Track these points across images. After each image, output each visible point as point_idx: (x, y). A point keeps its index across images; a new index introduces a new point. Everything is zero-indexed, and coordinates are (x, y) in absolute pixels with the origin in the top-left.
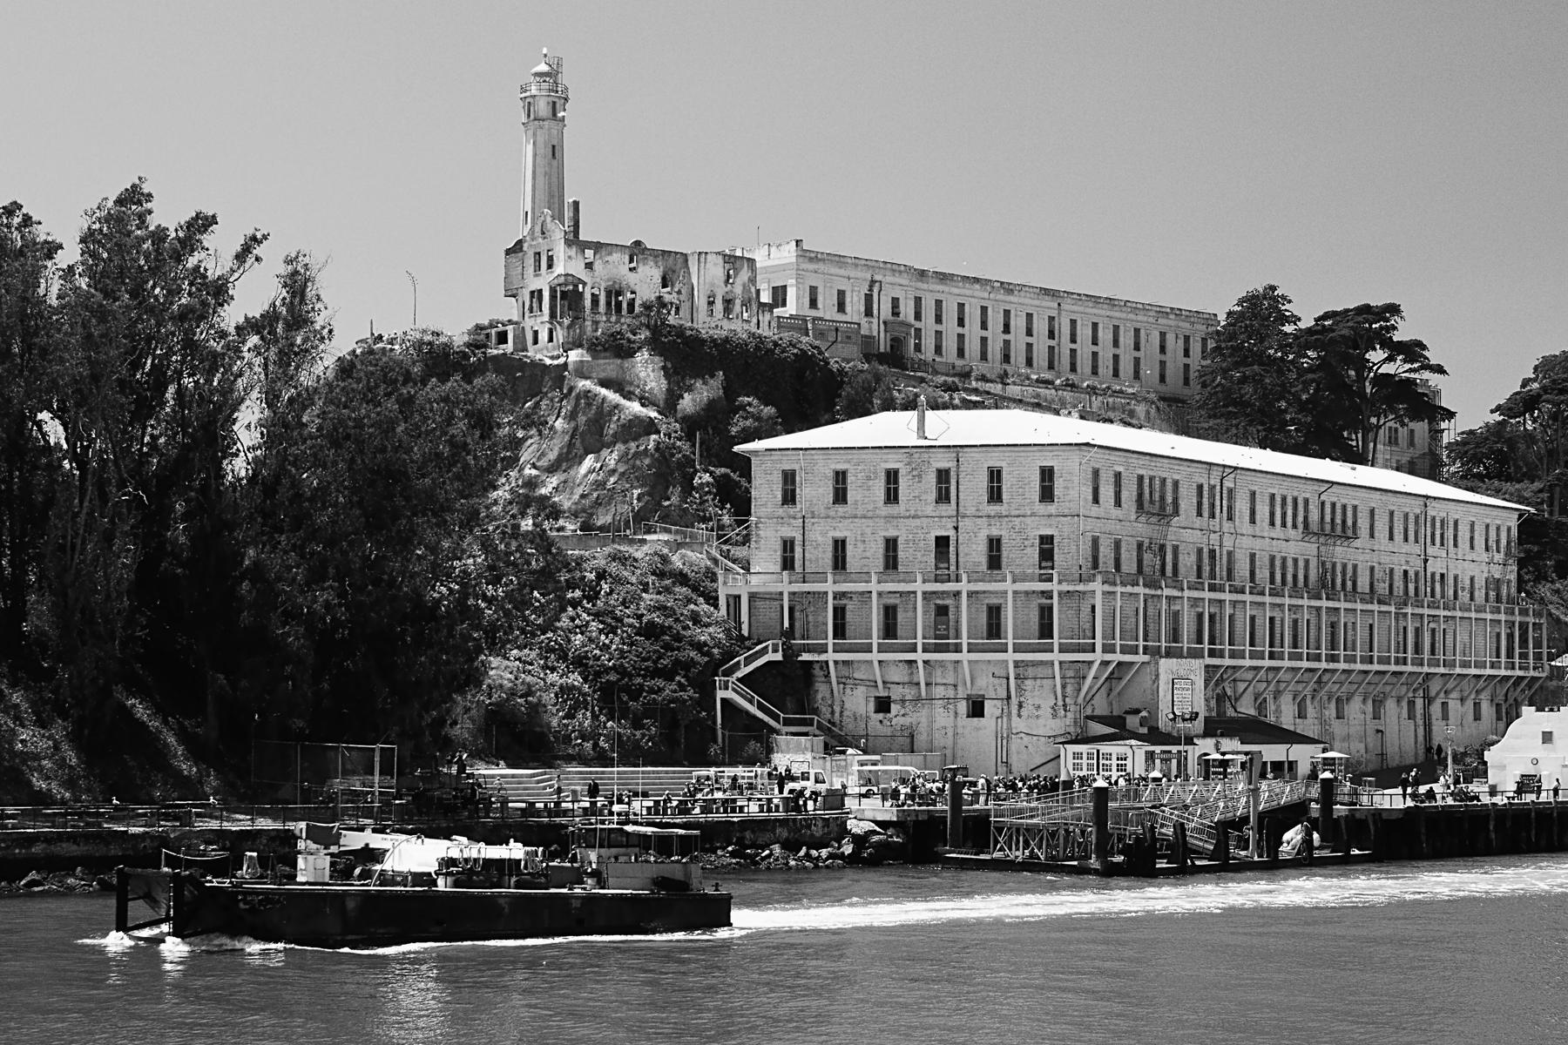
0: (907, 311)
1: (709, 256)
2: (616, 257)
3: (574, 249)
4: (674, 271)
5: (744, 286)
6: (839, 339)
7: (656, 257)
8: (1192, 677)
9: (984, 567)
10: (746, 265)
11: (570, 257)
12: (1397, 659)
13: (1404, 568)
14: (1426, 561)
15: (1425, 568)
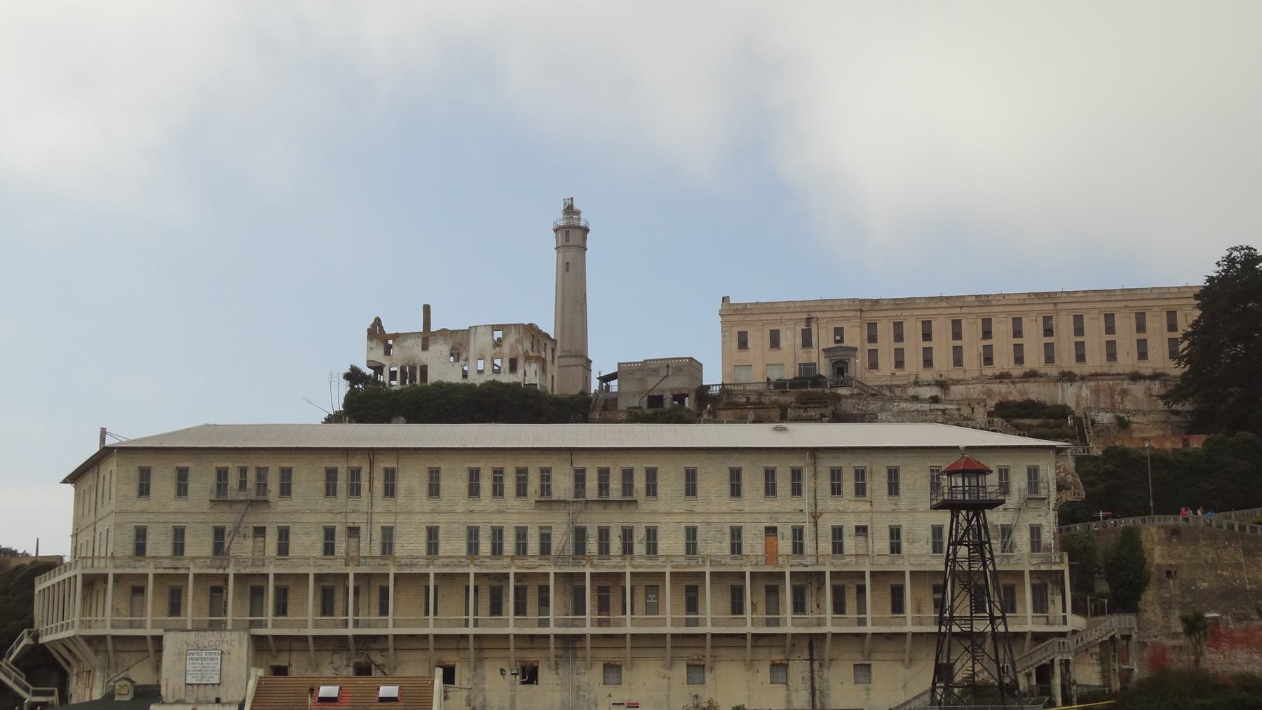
0: (854, 337)
1: (478, 329)
2: (410, 342)
3: (375, 342)
4: (461, 345)
5: (511, 346)
6: (671, 373)
7: (446, 336)
8: (225, 648)
9: (888, 551)
10: (513, 331)
11: (371, 348)
12: (82, 622)
13: (768, 525)
14: (815, 516)
15: (816, 525)
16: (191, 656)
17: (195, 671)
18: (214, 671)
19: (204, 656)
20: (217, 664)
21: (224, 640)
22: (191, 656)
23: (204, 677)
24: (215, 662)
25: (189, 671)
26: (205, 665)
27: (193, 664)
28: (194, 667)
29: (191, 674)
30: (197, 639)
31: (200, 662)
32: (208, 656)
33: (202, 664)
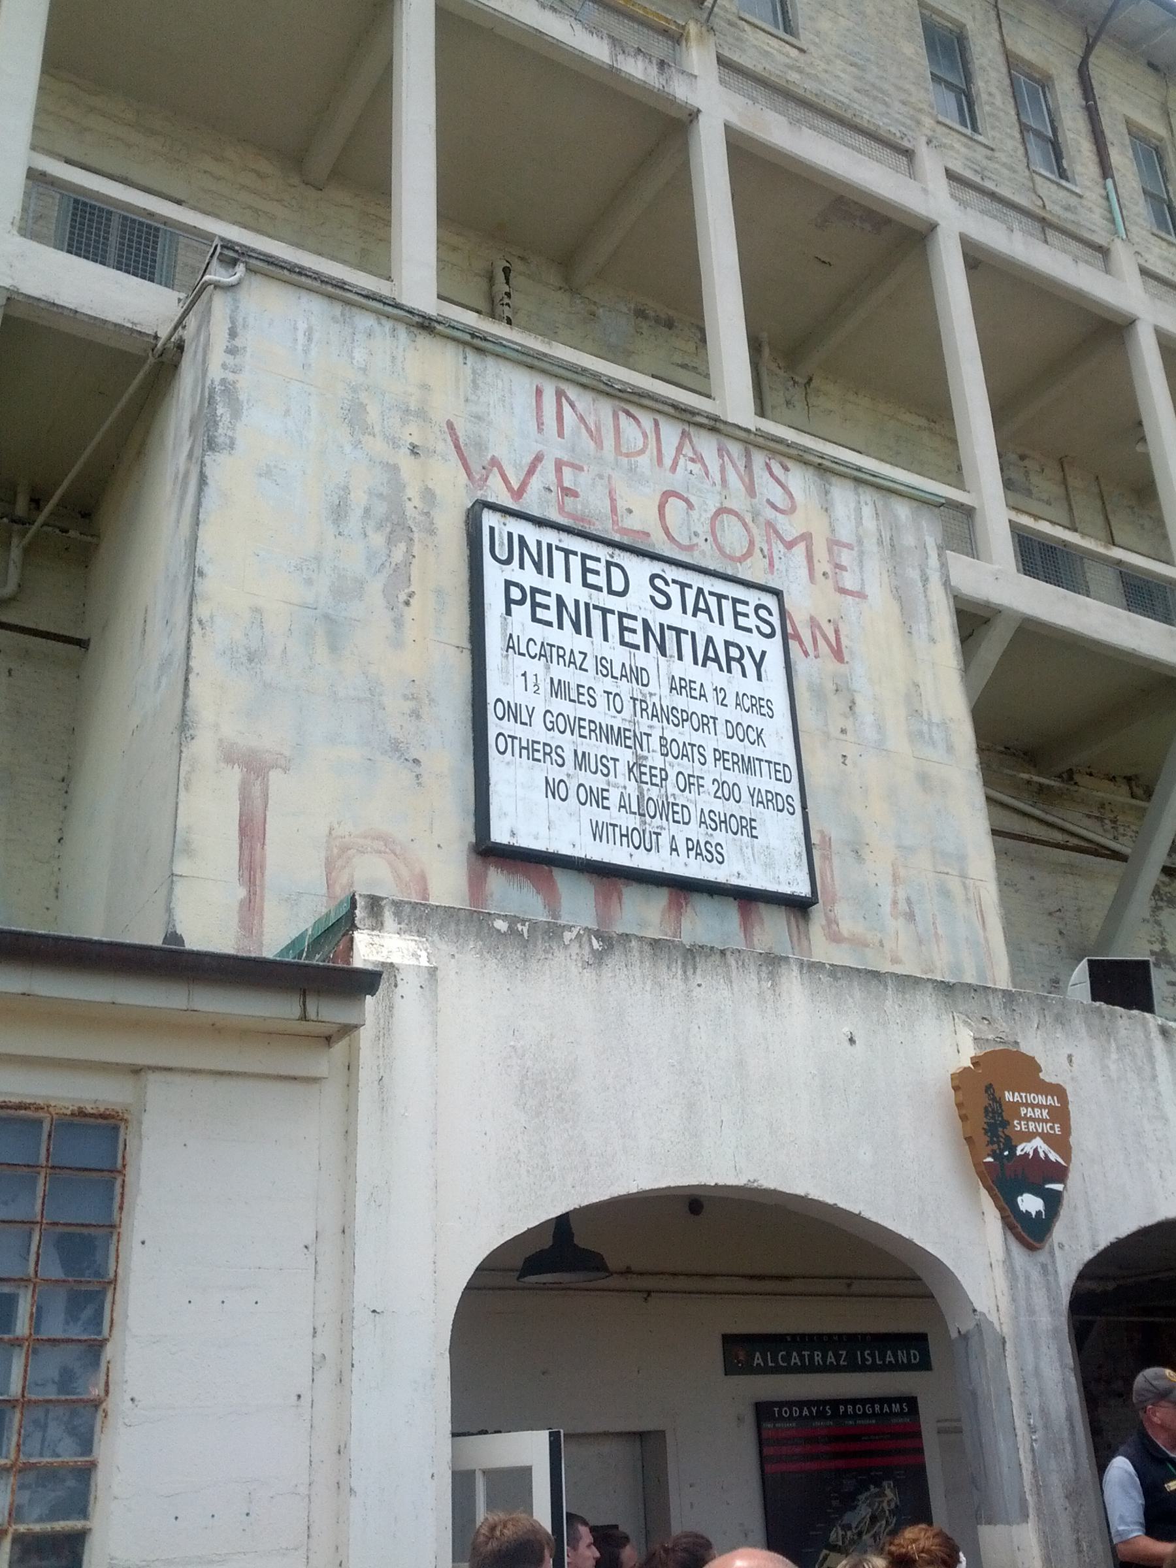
16: (529, 577)
17: (575, 726)
18: (748, 765)
19: (639, 601)
20: (759, 705)
21: (790, 527)
22: (529, 577)
23: (667, 809)
24: (736, 683)
25: (512, 712)
26: (660, 692)
27: (546, 652)
28: (558, 689)
29: (530, 749)
30: (555, 450)
31: (618, 655)
32: (673, 616)
33: (636, 675)
